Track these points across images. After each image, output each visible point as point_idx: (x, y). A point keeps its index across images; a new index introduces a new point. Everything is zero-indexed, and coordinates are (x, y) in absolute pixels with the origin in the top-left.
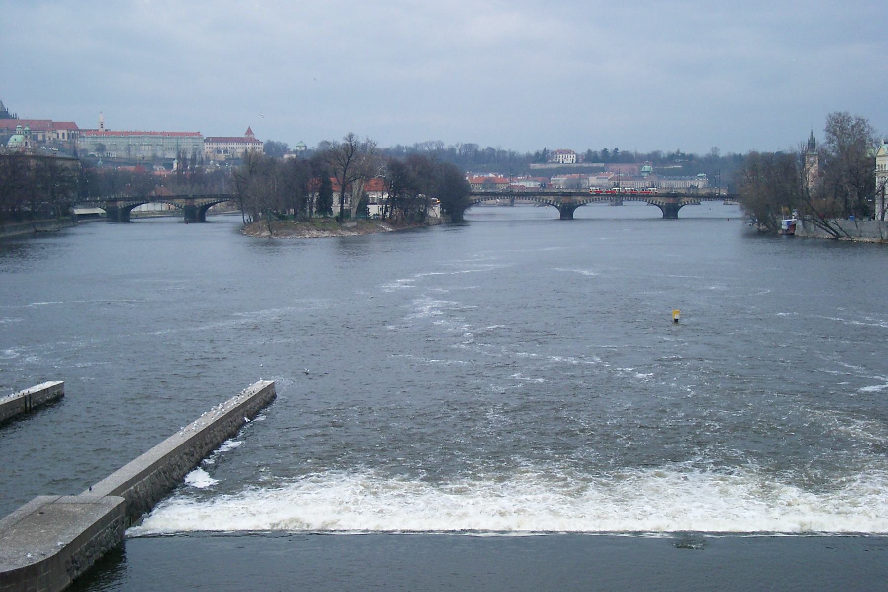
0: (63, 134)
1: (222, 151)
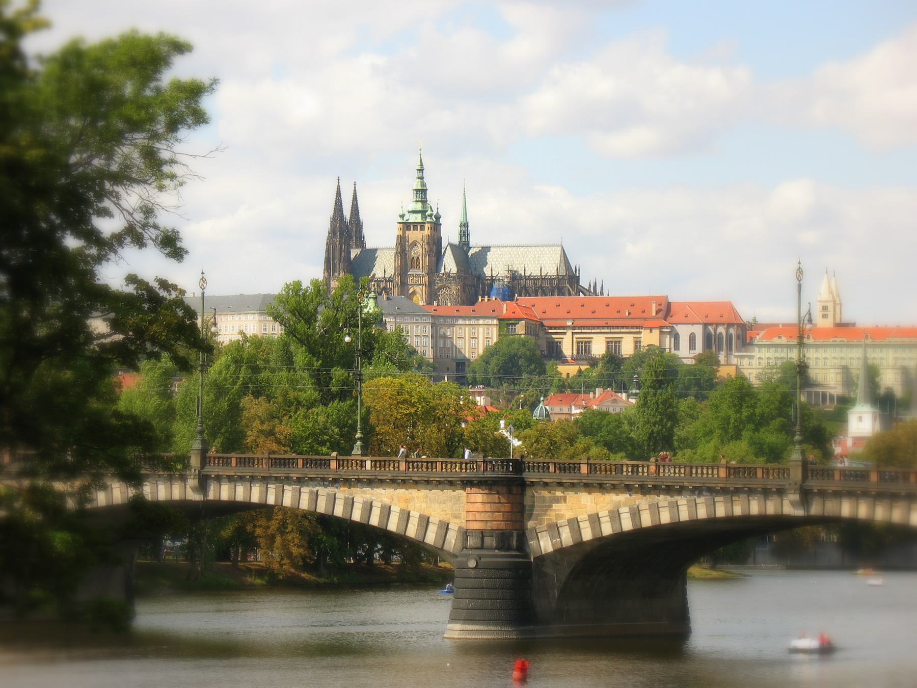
0: (692, 338)
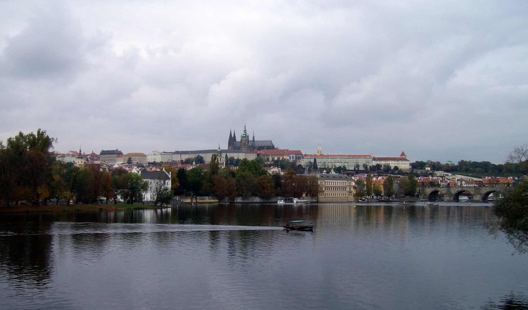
0: (293, 157)
1: (383, 166)
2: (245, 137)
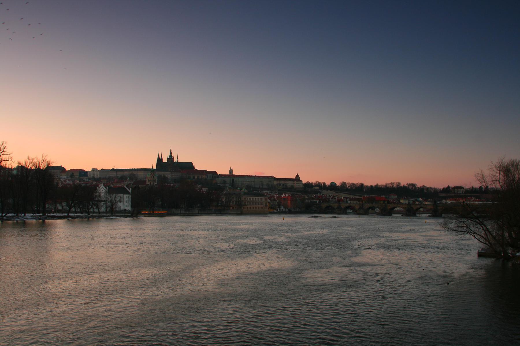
0: (210, 176)
1: (282, 185)
2: (171, 158)
